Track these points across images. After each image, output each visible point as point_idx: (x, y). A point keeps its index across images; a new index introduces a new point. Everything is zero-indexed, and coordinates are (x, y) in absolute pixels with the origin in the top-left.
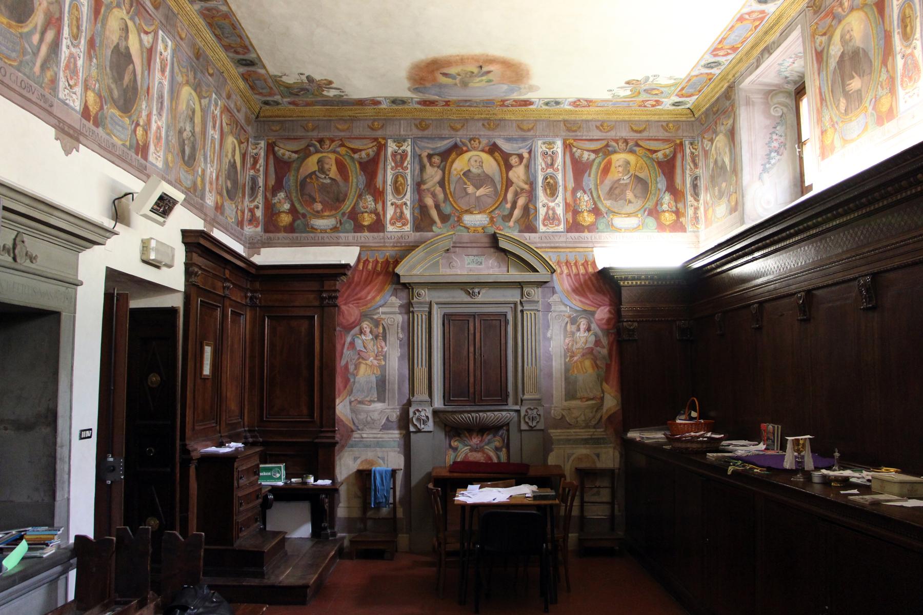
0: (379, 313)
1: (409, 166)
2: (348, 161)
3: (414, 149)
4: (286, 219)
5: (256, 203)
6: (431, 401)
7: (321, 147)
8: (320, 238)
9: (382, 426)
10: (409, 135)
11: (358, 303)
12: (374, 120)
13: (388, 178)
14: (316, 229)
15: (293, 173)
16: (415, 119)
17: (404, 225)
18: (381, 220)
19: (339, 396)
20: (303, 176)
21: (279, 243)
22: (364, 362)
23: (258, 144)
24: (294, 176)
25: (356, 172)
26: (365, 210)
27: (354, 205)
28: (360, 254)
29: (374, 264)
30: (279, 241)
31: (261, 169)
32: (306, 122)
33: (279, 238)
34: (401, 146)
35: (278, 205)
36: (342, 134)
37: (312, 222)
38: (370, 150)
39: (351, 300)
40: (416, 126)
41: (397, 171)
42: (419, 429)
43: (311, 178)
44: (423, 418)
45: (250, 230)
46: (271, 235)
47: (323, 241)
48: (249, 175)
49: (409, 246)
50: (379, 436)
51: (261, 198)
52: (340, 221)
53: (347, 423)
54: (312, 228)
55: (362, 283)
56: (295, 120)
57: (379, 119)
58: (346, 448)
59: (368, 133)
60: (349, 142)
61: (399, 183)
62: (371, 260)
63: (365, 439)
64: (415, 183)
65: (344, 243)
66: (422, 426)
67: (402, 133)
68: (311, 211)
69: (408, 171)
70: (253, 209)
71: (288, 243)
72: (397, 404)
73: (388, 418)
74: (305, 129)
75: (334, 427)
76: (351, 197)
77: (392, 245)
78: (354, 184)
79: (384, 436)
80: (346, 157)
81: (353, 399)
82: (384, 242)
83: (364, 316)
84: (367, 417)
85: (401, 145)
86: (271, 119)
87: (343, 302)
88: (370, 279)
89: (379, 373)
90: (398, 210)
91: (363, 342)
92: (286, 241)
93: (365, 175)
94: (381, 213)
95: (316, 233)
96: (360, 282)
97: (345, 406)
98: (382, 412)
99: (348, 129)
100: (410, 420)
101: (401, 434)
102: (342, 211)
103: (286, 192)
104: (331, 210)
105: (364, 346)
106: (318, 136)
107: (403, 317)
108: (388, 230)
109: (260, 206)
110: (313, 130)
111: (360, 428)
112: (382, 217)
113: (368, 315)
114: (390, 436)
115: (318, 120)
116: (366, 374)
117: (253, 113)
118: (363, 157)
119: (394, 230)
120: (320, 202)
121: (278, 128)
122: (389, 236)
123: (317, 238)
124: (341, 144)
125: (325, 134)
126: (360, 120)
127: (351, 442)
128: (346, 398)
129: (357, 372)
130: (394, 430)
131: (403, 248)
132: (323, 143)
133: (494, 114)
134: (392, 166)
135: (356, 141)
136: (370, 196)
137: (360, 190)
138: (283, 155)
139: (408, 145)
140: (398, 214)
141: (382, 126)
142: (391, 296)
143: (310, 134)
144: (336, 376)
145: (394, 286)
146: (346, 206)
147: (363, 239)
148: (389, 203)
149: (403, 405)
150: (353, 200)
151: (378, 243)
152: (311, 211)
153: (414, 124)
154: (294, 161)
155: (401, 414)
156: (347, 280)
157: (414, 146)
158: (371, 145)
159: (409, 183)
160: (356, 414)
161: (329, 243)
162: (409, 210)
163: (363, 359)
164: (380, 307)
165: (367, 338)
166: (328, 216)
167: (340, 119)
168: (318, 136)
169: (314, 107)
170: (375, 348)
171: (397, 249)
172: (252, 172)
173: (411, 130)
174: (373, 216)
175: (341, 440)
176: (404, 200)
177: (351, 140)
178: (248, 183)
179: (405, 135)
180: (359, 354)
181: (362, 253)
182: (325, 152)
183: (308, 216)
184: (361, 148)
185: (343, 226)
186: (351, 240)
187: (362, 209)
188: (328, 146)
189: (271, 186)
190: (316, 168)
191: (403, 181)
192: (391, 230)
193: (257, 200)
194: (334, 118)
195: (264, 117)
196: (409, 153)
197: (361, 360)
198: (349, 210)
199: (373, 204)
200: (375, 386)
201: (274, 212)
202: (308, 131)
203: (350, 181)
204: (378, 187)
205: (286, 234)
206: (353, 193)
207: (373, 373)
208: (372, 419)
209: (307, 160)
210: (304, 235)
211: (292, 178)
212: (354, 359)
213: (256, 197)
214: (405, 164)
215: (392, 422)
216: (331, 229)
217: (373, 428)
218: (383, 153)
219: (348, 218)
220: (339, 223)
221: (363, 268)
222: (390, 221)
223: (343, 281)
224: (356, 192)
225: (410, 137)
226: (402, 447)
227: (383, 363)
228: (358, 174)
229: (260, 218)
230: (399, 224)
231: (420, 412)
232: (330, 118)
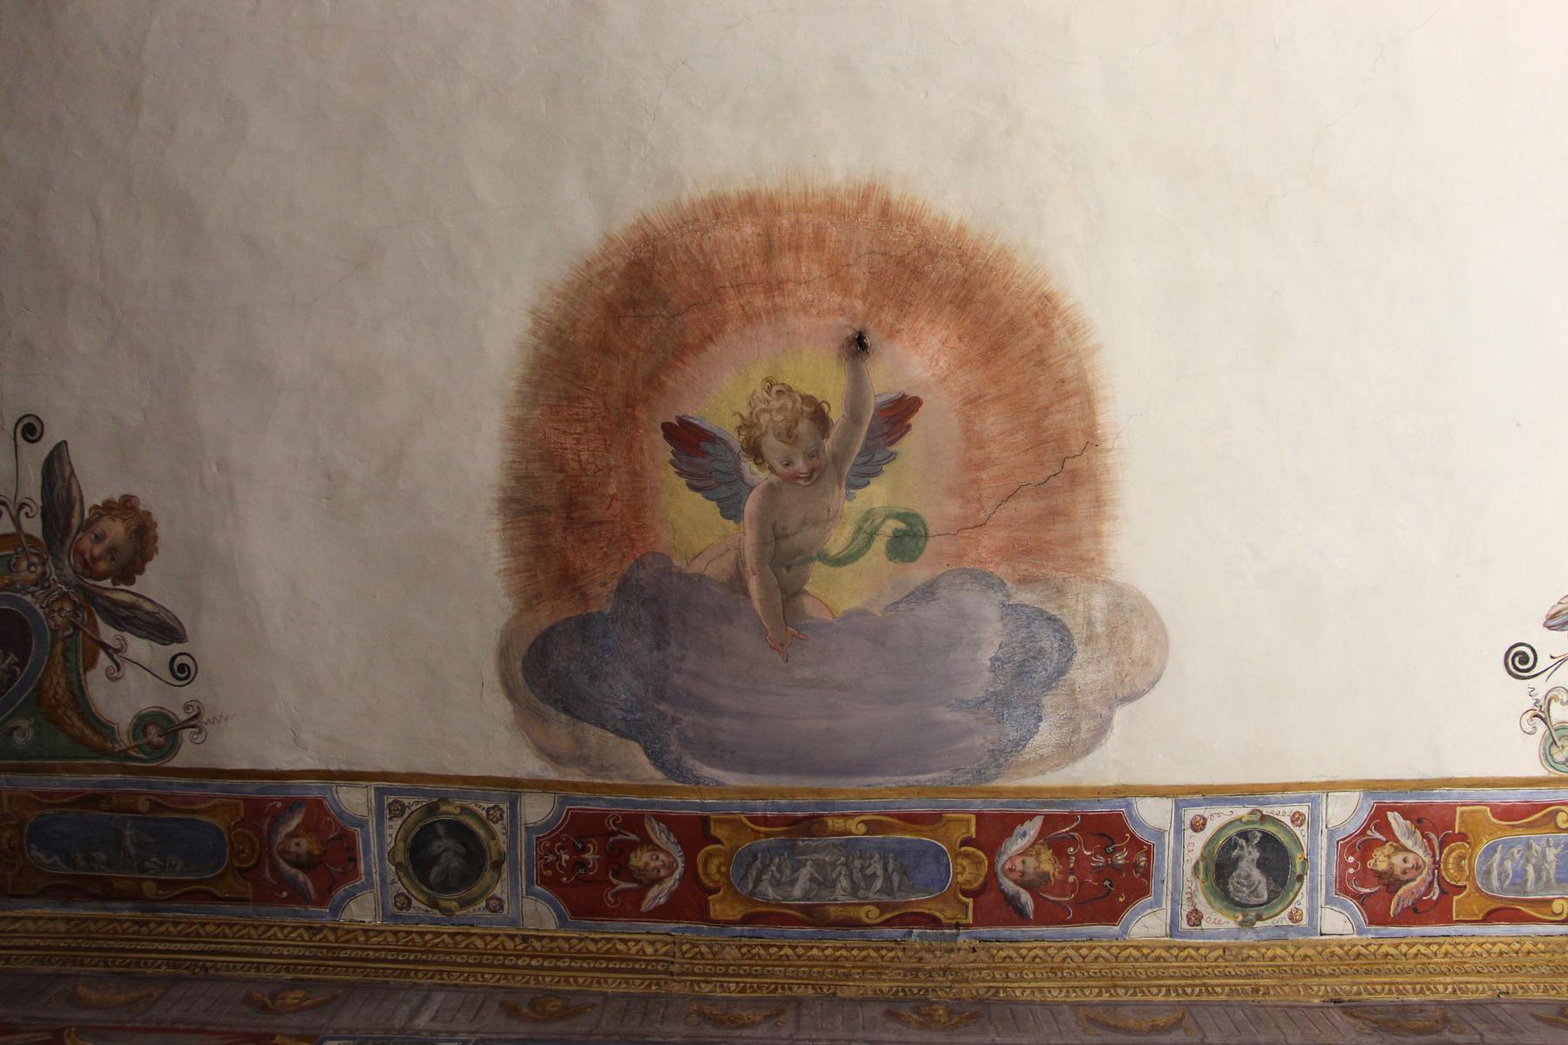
133: (945, 971)
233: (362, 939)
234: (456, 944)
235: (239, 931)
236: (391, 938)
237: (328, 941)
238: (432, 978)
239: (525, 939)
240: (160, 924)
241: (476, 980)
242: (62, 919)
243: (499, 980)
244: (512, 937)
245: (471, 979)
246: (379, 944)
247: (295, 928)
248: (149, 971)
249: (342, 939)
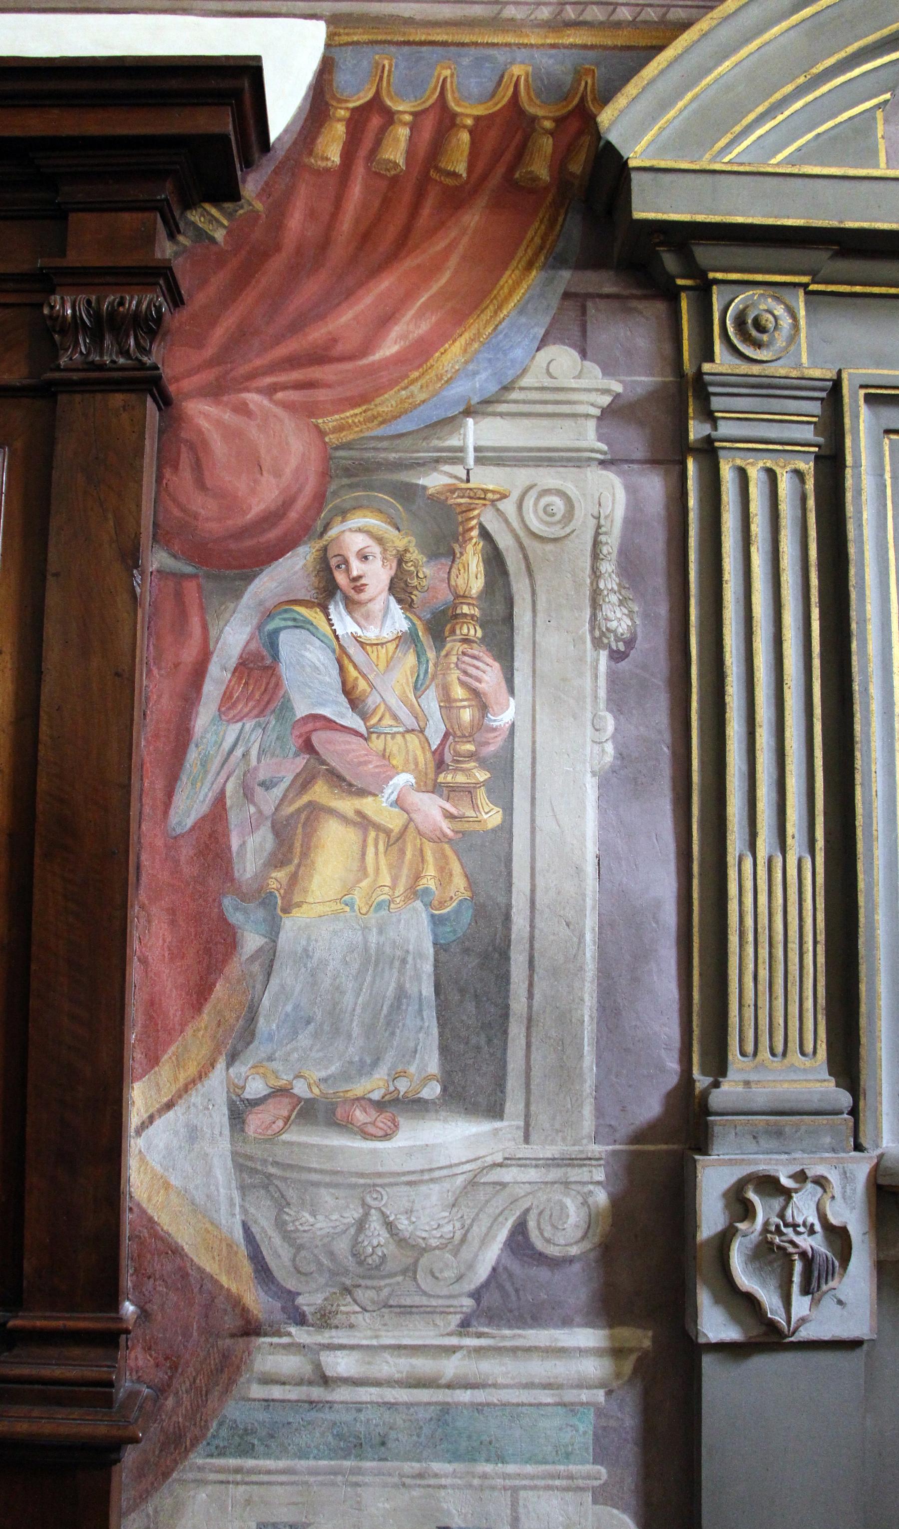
0: (456, 456)
6: (854, 1112)
9: (476, 1295)
11: (310, 385)
19: (153, 1060)
22: (347, 805)
28: (327, 67)
29: (427, 134)
39: (257, 361)
42: (772, 1326)
44: (805, 1242)
50: (451, 1367)
53: (210, 1266)
55: (338, 252)
58: (197, 1459)
62: (403, 107)
63: (342, 1394)
66: (801, 1305)
72: (588, 1123)
73: (520, 1229)
75: (114, 1303)
79: (489, 1367)
81: (256, 1088)
83: (348, 472)
84: (361, 1225)
87: (208, 376)
88: (392, 231)
89: (459, 882)
91: (342, 658)
96: (324, 244)
97: (193, 1134)
98: (473, 1183)
100: (706, 1260)
101: (617, 1352)
105: (348, 691)
107: (631, 490)
111: (309, 1302)
113: (380, 466)
114: (539, 1369)
116: (358, 897)
127: (233, 1410)
128: (201, 1076)
129: (294, 879)
130: (566, 1322)
142: (543, 343)
144: (135, 911)
145: (566, 274)
149: (639, 1137)
155: (616, 1202)
156: (230, 232)
160: (281, 1203)
163: (336, 779)
164: (468, 412)
165: (371, 633)
170: (431, 702)
175: (161, 1390)
180: (308, 747)
181: (346, 59)
197: (320, 792)
200: (428, 990)
207: (415, 892)
208: (402, 1242)
212: (267, 785)
215: (555, 1263)
217: (406, 1311)
221: (348, 154)
223: (201, 235)
226: (630, 1453)
227: (492, 817)
231: (787, 1194)
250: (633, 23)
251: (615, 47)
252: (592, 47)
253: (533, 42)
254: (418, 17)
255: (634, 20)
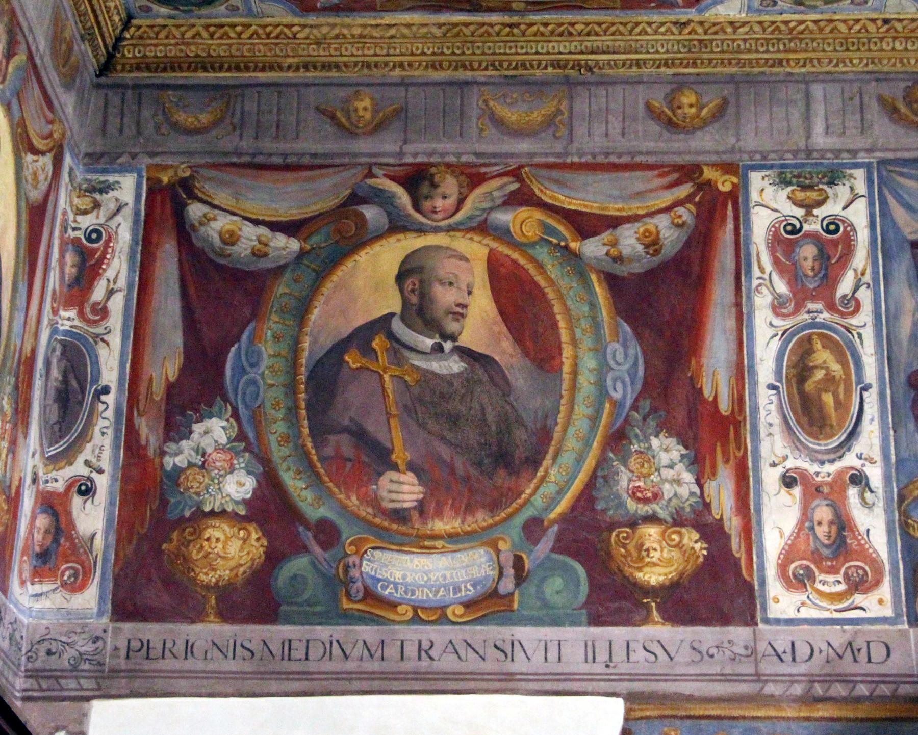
1: (865, 296)
2: (553, 271)
3: (886, 213)
4: (234, 548)
5: (79, 468)
7: (417, 206)
8: (411, 650)
10: (854, 153)
12: (679, 85)
13: (759, 351)
14: (392, 605)
15: (273, 324)
16: (881, 78)
17: (858, 585)
18: (737, 562)
20: (327, 342)
21: (182, 674)
23: (105, 188)
24: (277, 338)
25: (596, 325)
26: (645, 509)
27: (593, 477)
30: (190, 664)
31: (117, 304)
32: (342, 93)
33: (189, 648)
34: (820, 203)
35: (194, 482)
36: (524, 146)
37: (366, 567)
38: (662, 222)
40: (891, 110)
41: (803, 317)
43: (368, 351)
45: (45, 604)
46: (152, 631)
47: (425, 664)
48: (55, 331)
49: (894, 698)
51: (107, 442)
52: (518, 563)
54: (370, 595)
56: (288, 85)
57: (701, 80)
59: (650, 145)
60: (557, 182)
61: (819, 375)
64: (902, 378)
65: (539, 677)
67: (820, 140)
68: (366, 512)
69: (865, 317)
70: (65, 495)
71: (241, 675)
74: (339, 125)
76: (572, 443)
77: (798, 690)
78: (586, 381)
80: (542, 254)
82: (758, 677)
85: (813, 195)
86: (169, 77)
90: (823, 513)
92: (231, 665)
93: (639, 336)
94: (733, 524)
95: (394, 622)
99: (550, 122)
102: (528, 513)
103: (236, 415)
104: (469, 509)
106: (401, 154)
108: (774, 611)
109: (102, 482)
110: (378, 127)
112: (736, 545)
115: (403, 83)
117: (92, 40)
118: (626, 252)
119: (805, 613)
120: (411, 467)
121: (205, 118)
122: (782, 645)
123: (392, 651)
124: (512, 193)
125: (440, 147)
126: (604, 82)
131: (862, 712)
132: (425, 189)
134: (778, 296)
135: (582, 178)
136: (672, 442)
137: (614, 415)
138: (230, 239)
139: (855, 197)
140: (821, 531)
141: (719, 114)
143: (363, 145)
146: (549, 489)
147: (639, 655)
148: (771, 477)
150: (580, 460)
151: (725, 678)
152: (366, 512)
153: (881, 99)
154: (279, 270)
157: (883, 203)
158: (667, 198)
159: (870, 373)
161: (457, 676)
162: (879, 510)
166: (452, 537)
167: (510, 81)
168: (401, 154)
169: (388, 19)
171: (823, 711)
172: (68, 319)
173: (864, 128)
174: (691, 538)
176: (850, 460)
177: (568, 176)
178: (48, 364)
179: (837, 153)
182: (436, 230)
183: (348, 534)
184: (614, 209)
185: (531, 588)
186: (574, 660)
187: (632, 505)
188: (451, 201)
189: (159, 390)
190: (392, 303)
191: (836, 368)
192: (791, 614)
193: (87, 453)
194: (480, 75)
195: (139, 68)
196: (863, 236)
198: (561, 507)
199: (688, 477)
201: (172, 516)
202: (349, 131)
203: (566, 368)
204: (707, 393)
205: (228, 630)
206: (580, 424)
209: (349, 264)
210: (323, 632)
211: (267, 349)
213: (84, 437)
214: (845, 287)
216: (469, 605)
218: (726, 235)
219: (553, 550)
220: (510, 572)
222: (783, 568)
224: (594, 420)
225: (863, 158)
228: (607, 331)
229: (99, 542)
230: (832, 583)
232: (462, 75)
233: (729, 30)
234: (821, 30)
235: (608, 28)
236: (757, 28)
237: (696, 33)
238: (804, 66)
239: (886, 21)
240: (531, 25)
241: (845, 66)
242: (434, 25)
243: (867, 65)
244: (873, 21)
245: (841, 65)
246: (747, 33)
247: (663, 24)
248: (538, 73)
249: (710, 31)
250: (870, 698)
251: (857, 719)
252: (838, 719)
253: (789, 715)
254: (696, 694)
255: (871, 694)
